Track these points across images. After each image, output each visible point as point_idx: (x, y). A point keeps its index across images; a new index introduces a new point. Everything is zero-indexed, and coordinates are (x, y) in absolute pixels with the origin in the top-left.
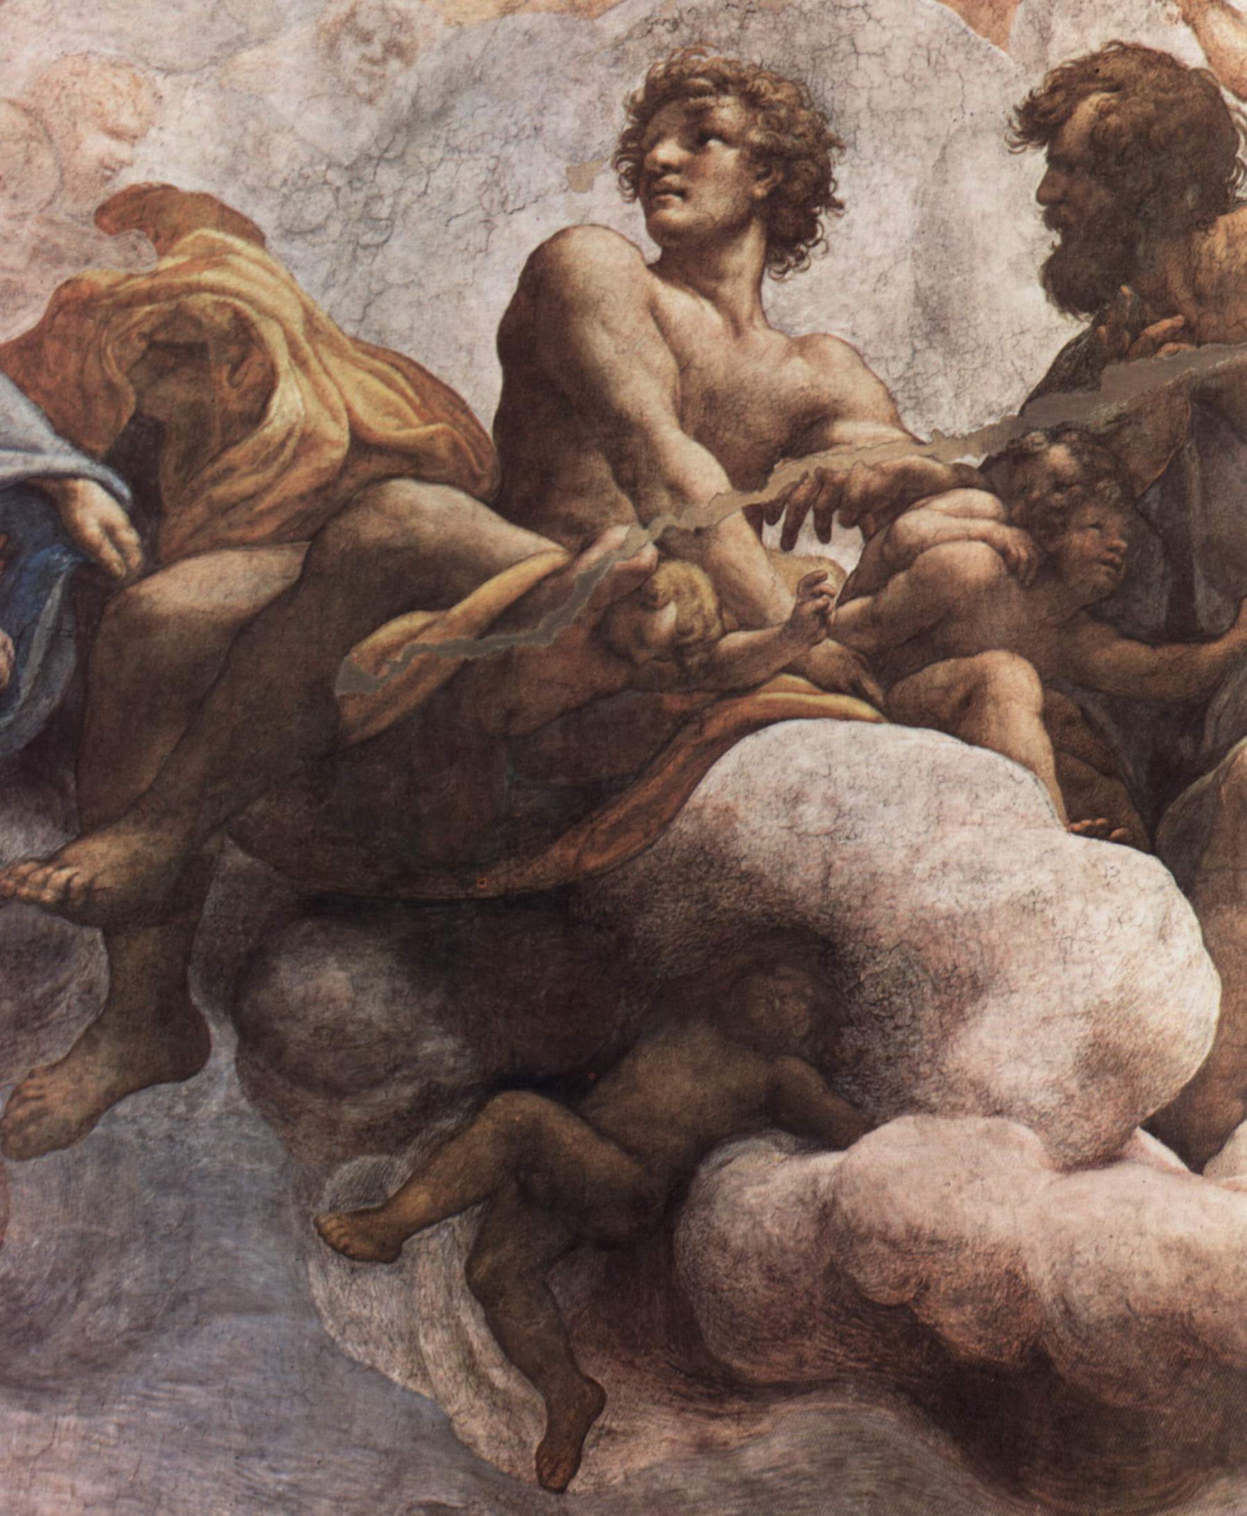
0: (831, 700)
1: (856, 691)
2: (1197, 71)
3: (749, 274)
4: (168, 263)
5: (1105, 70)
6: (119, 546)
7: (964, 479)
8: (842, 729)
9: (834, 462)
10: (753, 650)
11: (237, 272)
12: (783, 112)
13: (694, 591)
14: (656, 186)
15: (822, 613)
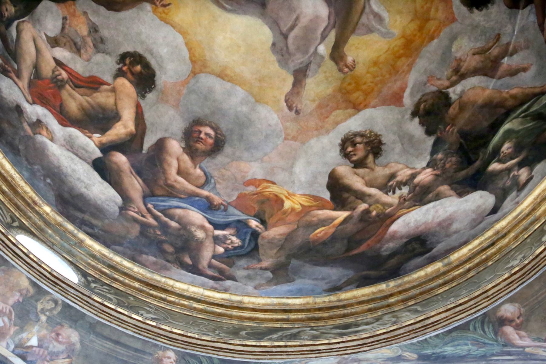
0: (411, 209)
1: (415, 206)
2: (437, 91)
3: (372, 162)
4: (258, 189)
5: (422, 100)
6: (260, 228)
7: (424, 169)
8: (414, 212)
9: (399, 178)
10: (392, 210)
11: (273, 189)
12: (369, 135)
13: (378, 207)
14: (349, 155)
15: (405, 200)
